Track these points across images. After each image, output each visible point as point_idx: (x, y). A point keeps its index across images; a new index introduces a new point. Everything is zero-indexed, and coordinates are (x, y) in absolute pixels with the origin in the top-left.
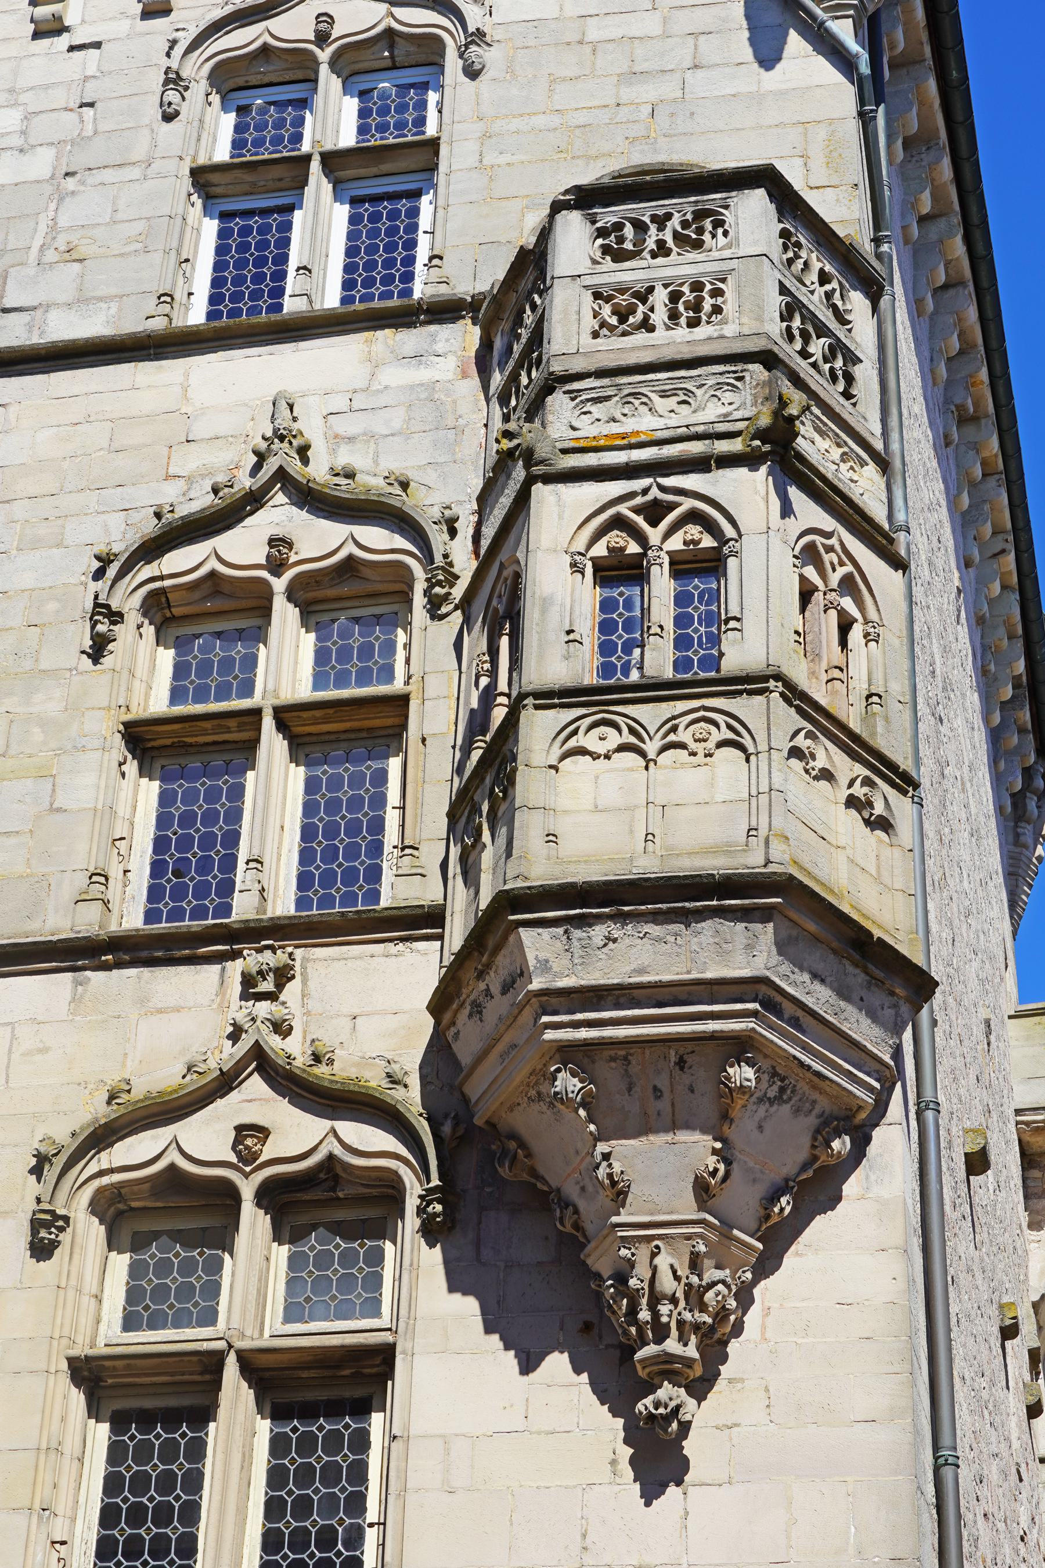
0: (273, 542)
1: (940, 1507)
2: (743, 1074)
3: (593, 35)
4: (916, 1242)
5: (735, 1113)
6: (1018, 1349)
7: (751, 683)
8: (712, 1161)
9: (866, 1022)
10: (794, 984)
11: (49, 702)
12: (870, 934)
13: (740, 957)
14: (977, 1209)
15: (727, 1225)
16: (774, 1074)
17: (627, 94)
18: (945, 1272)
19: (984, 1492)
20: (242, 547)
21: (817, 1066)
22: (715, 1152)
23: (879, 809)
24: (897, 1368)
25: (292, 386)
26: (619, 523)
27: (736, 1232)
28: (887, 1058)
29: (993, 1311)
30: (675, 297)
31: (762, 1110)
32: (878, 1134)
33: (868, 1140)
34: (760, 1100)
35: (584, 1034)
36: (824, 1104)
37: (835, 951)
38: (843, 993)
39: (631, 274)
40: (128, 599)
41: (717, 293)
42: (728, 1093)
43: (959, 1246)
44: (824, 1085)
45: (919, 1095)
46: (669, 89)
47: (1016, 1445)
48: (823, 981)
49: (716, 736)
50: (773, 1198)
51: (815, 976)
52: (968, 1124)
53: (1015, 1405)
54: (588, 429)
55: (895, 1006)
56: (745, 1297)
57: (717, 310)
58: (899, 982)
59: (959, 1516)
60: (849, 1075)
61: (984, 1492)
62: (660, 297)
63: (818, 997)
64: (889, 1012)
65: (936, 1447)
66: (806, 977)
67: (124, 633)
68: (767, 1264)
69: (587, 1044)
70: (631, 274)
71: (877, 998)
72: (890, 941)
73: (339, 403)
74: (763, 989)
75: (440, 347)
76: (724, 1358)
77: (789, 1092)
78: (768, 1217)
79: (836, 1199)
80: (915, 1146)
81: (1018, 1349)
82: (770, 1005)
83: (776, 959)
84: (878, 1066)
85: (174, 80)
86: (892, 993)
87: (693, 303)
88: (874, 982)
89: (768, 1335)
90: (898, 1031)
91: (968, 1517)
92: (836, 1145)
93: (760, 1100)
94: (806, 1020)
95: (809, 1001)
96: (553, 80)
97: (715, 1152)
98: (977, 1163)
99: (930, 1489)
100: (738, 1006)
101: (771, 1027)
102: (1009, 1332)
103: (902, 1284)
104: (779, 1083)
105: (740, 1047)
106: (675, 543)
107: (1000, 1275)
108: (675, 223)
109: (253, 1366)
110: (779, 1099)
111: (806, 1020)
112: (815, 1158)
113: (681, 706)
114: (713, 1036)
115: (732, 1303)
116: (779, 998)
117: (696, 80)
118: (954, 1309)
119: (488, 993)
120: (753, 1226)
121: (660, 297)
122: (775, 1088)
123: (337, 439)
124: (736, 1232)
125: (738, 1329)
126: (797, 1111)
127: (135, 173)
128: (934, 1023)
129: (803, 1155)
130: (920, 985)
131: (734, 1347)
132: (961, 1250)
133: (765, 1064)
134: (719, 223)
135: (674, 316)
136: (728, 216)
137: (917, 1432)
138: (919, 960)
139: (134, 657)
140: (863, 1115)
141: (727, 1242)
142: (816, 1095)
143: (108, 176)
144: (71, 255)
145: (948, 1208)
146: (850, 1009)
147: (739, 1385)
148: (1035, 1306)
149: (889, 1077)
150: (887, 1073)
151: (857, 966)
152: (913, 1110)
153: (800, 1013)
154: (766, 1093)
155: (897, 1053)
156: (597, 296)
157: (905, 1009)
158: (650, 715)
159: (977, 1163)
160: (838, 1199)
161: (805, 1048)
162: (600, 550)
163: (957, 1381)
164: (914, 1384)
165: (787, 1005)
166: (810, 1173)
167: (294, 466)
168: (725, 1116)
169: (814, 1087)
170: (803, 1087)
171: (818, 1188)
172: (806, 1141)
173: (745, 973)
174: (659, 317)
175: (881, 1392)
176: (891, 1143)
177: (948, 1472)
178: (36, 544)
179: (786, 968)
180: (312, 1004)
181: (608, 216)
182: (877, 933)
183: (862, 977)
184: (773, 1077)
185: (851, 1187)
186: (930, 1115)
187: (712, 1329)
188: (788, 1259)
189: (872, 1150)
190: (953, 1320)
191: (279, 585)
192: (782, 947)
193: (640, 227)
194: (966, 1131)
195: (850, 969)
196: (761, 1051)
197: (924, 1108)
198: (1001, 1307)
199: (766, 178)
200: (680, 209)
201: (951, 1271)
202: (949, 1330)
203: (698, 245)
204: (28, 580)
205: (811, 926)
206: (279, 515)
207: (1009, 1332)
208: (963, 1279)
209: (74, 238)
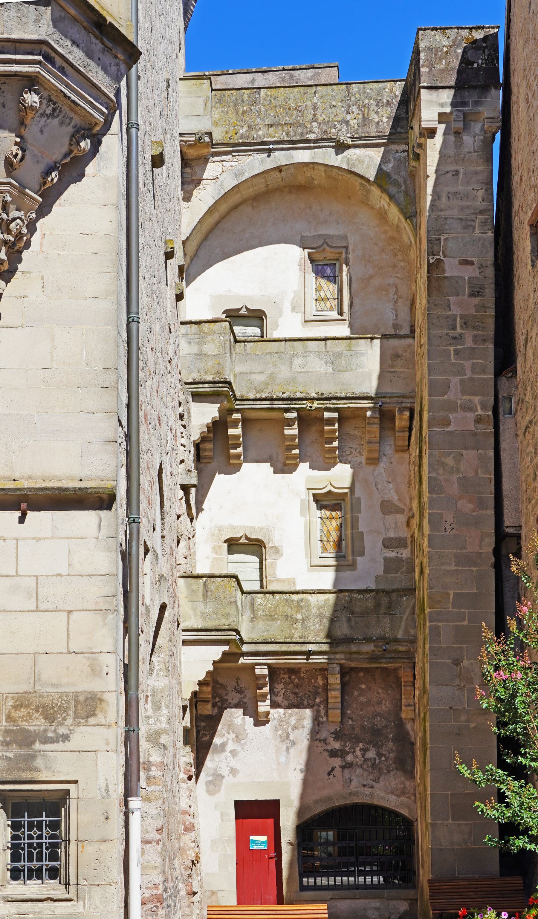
1: (129, 343)
2: (32, 98)
4: (123, 202)
5: (28, 122)
6: (174, 264)
8: (14, 149)
9: (101, 73)
10: (62, 46)
12: (105, 20)
13: (32, 27)
14: (156, 187)
15: (23, 186)
16: (50, 100)
18: (138, 220)
19: (152, 337)
21: (73, 97)
22: (16, 143)
24: (110, 270)
27: (27, 191)
28: (112, 96)
29: (162, 244)
32: (105, 140)
33: (100, 143)
34: (42, 115)
36: (77, 120)
37: (85, 28)
38: (89, 54)
42: (24, 109)
43: (145, 206)
44: (77, 109)
45: (128, 120)
47: (169, 314)
48: (78, 46)
50: (48, 173)
51: (74, 43)
52: (154, 139)
53: (170, 294)
55: (117, 65)
56: (32, 228)
58: (121, 51)
59: (138, 348)
60: (91, 104)
61: (152, 337)
63: (76, 56)
64: (114, 68)
65: (128, 312)
66: (69, 43)
68: (44, 210)
71: (108, 59)
72: (117, 25)
74: (45, 48)
76: (20, 260)
77: (58, 111)
78: (45, 183)
79: (81, 176)
80: (125, 148)
81: (174, 264)
82: (47, 58)
83: (52, 30)
84: (107, 100)
86: (116, 57)
88: (107, 49)
89: (44, 249)
90: (118, 80)
91: (143, 349)
92: (83, 144)
93: (42, 115)
94: (68, 69)
95: (70, 57)
97: (16, 143)
98: (158, 161)
99: (124, 334)
100: (30, 57)
101: (49, 72)
102: (169, 255)
103: (114, 225)
104: (52, 106)
105: (31, 82)
107: (166, 224)
110: (52, 115)
111: (68, 69)
112: (71, 151)
114: (15, 75)
115: (25, 231)
116: (53, 54)
118: (141, 240)
120: (37, 188)
122: (50, 108)
124: (27, 191)
125: (28, 245)
126: (62, 123)
128: (139, 78)
129: (65, 149)
130: (133, 54)
131: (25, 254)
132: (147, 209)
133: (45, 94)
137: (119, 304)
138: (131, 38)
140: (98, 128)
141: (22, 196)
142: (72, 115)
145: (141, 185)
146: (93, 64)
147: (28, 275)
148: (184, 242)
149: (113, 107)
150: (112, 104)
151: (97, 38)
152: (125, 127)
153: (65, 65)
154: (45, 111)
155: (118, 93)
157: (123, 67)
159: (158, 161)
160: (83, 175)
161: (67, 86)
163: (141, 279)
164: (119, 279)
165: (58, 59)
166: (68, 160)
168: (22, 123)
169: (72, 110)
170: (65, 109)
171: (72, 168)
172: (66, 140)
173: (35, 37)
175: (102, 282)
176: (112, 144)
177: (134, 325)
179: (58, 36)
182: (109, 19)
183: (100, 46)
184: (49, 102)
185: (90, 169)
186: (133, 131)
187: (14, 244)
188: (55, 208)
189: (102, 148)
190: (141, 246)
192: (55, 22)
194: (153, 143)
195: (94, 40)
196: (43, 86)
197: (131, 126)
198: (166, 242)
201: (141, 220)
202: (138, 251)
205: (72, 11)
207: (169, 255)
208: (147, 225)
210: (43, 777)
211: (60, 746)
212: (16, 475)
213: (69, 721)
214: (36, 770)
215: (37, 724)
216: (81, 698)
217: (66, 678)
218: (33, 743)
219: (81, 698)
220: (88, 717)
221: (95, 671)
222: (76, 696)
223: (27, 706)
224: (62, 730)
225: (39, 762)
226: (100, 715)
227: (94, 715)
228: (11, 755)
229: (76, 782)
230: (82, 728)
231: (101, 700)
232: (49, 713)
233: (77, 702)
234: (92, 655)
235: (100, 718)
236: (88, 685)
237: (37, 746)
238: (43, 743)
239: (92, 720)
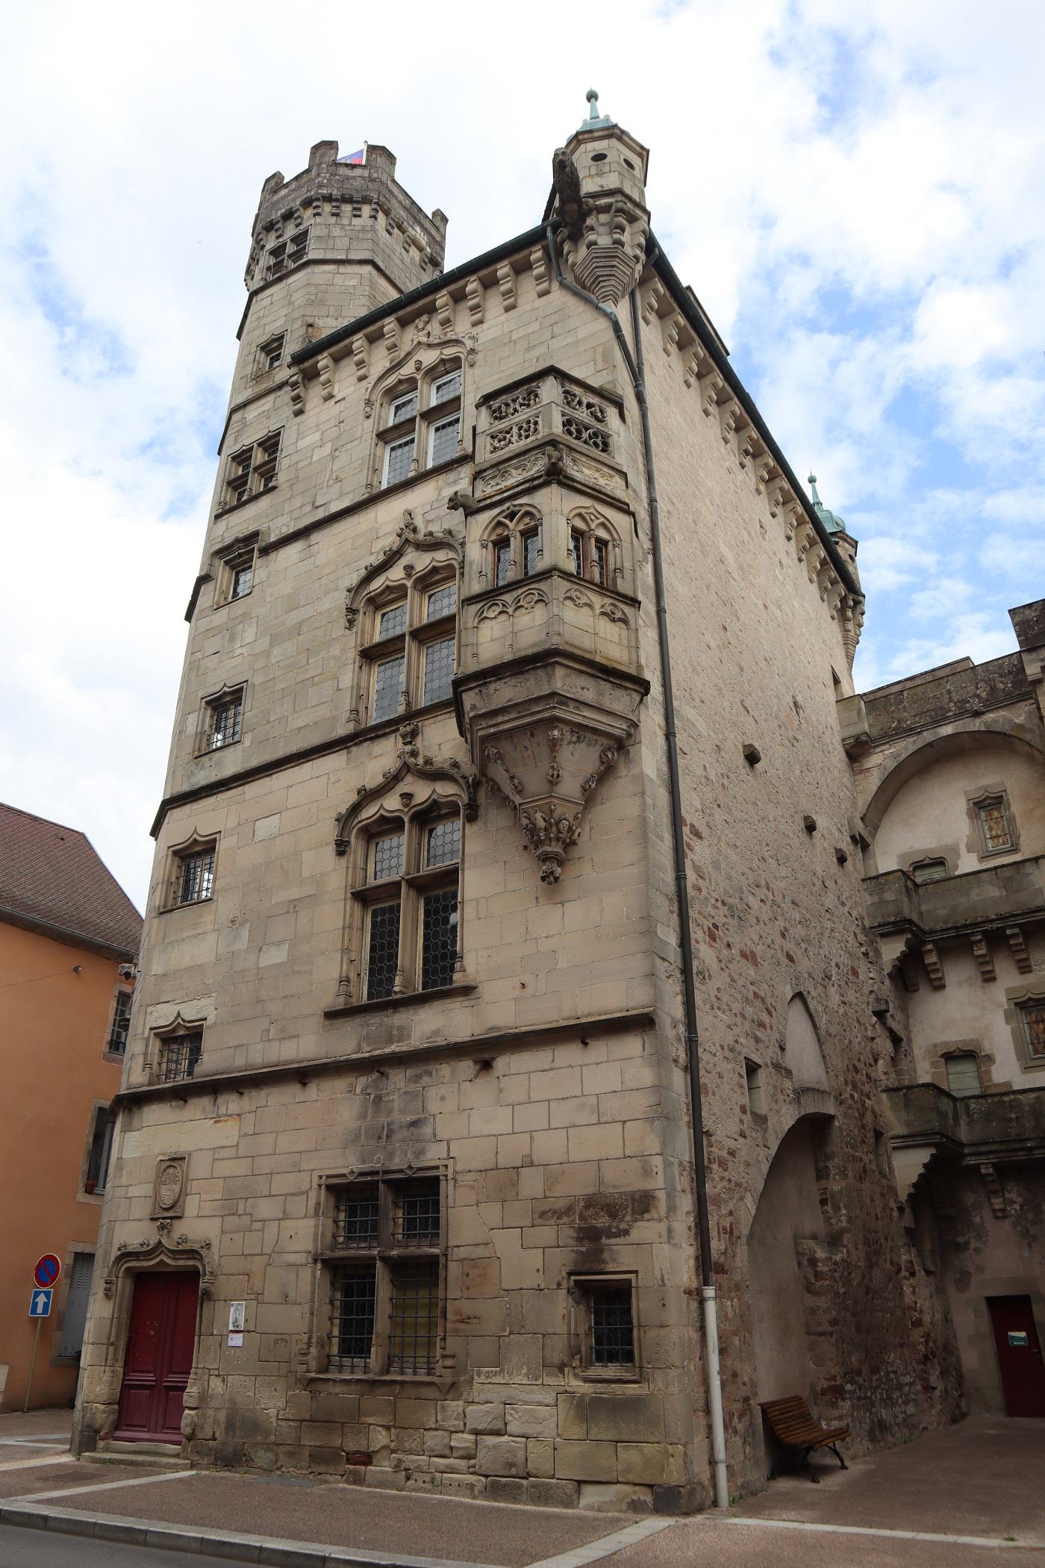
0: (405, 568)
3: (515, 337)
7: (545, 575)
11: (335, 651)
17: (527, 356)
20: (396, 574)
23: (619, 615)
25: (409, 507)
26: (500, 524)
30: (520, 428)
31: (571, 747)
35: (492, 730)
39: (503, 425)
40: (360, 605)
41: (536, 423)
46: (543, 349)
49: (536, 598)
54: (489, 490)
57: (536, 430)
62: (515, 430)
67: (360, 617)
69: (494, 734)
70: (503, 425)
73: (428, 508)
85: (369, 403)
87: (528, 428)
96: (500, 360)
106: (521, 527)
108: (520, 400)
109: (411, 883)
113: (520, 591)
121: (515, 430)
123: (428, 522)
127: (357, 442)
134: (536, 396)
135: (520, 436)
136: (539, 391)
139: (363, 625)
143: (349, 446)
144: (338, 480)
156: (493, 437)
158: (508, 598)
162: (494, 537)
167: (411, 536)
174: (515, 438)
178: (327, 593)
180: (426, 743)
181: (495, 404)
191: (409, 584)
193: (507, 405)
199: (552, 371)
200: (520, 393)
203: (528, 406)
204: (327, 606)
206: (411, 557)
210: (610, 1267)
211: (621, 1240)
212: (580, 1014)
213: (628, 1218)
214: (605, 1262)
215: (603, 1221)
216: (637, 1197)
217: (622, 1179)
218: (601, 1238)
219: (637, 1197)
220: (642, 1213)
221: (647, 1172)
222: (632, 1194)
223: (595, 1206)
224: (623, 1226)
225: (606, 1255)
226: (653, 1211)
227: (648, 1211)
228: (584, 1249)
229: (636, 1272)
230: (639, 1223)
231: (653, 1197)
232: (612, 1210)
233: (633, 1200)
234: (643, 1157)
235: (654, 1214)
236: (639, 1185)
237: (604, 1240)
238: (608, 1237)
239: (646, 1216)
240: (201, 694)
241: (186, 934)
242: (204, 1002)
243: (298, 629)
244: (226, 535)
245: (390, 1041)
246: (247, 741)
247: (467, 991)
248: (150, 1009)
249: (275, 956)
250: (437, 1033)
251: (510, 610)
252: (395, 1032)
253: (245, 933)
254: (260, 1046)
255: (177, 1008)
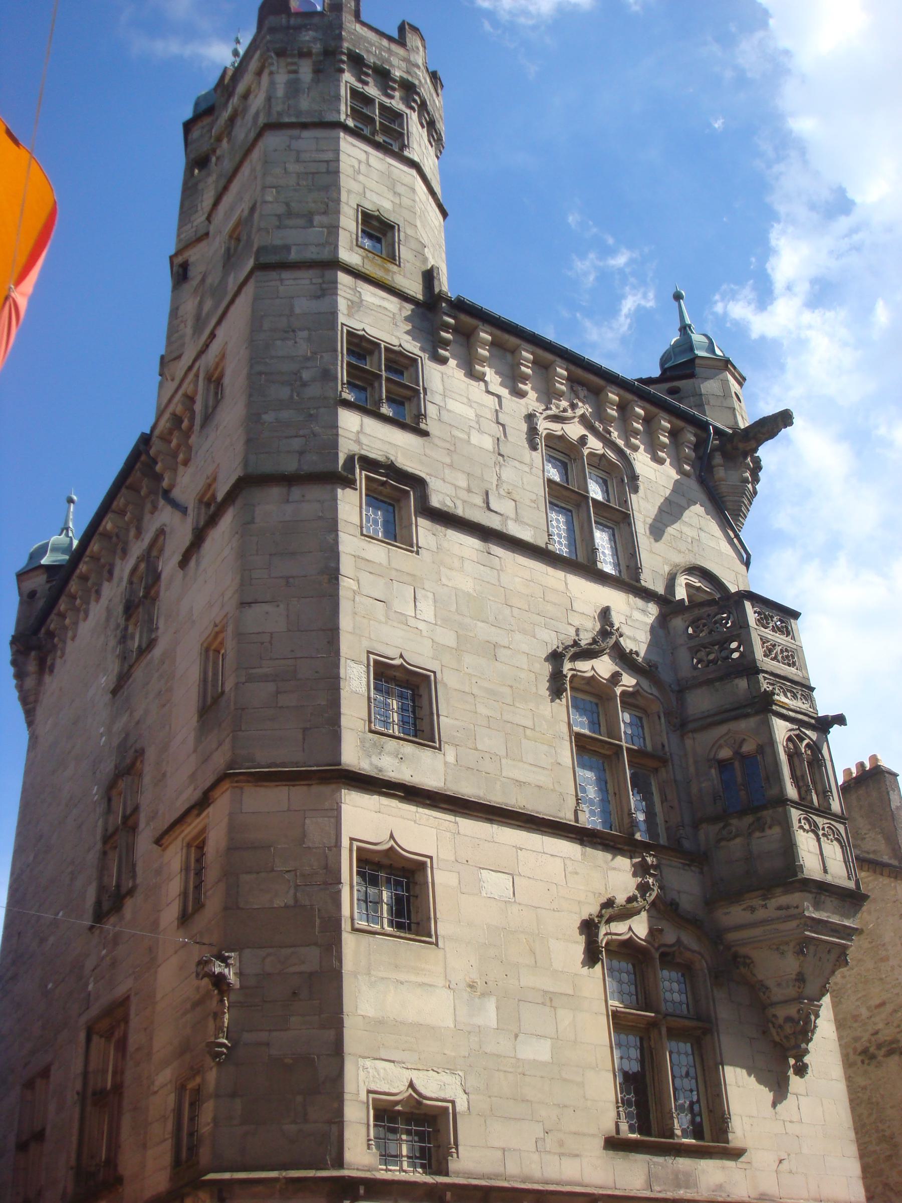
75: (650, 610)
117: (702, 534)
119: (765, 906)
204: (525, 647)
209: (510, 488)
240: (366, 644)
241: (402, 977)
242: (446, 1078)
243: (492, 650)
244: (364, 440)
245: (678, 1186)
246: (450, 754)
247: (736, 1154)
248: (361, 1062)
249: (537, 1051)
250: (720, 1187)
251: (821, 833)
252: (681, 1176)
253: (491, 1005)
254: (535, 1157)
255: (407, 1075)
